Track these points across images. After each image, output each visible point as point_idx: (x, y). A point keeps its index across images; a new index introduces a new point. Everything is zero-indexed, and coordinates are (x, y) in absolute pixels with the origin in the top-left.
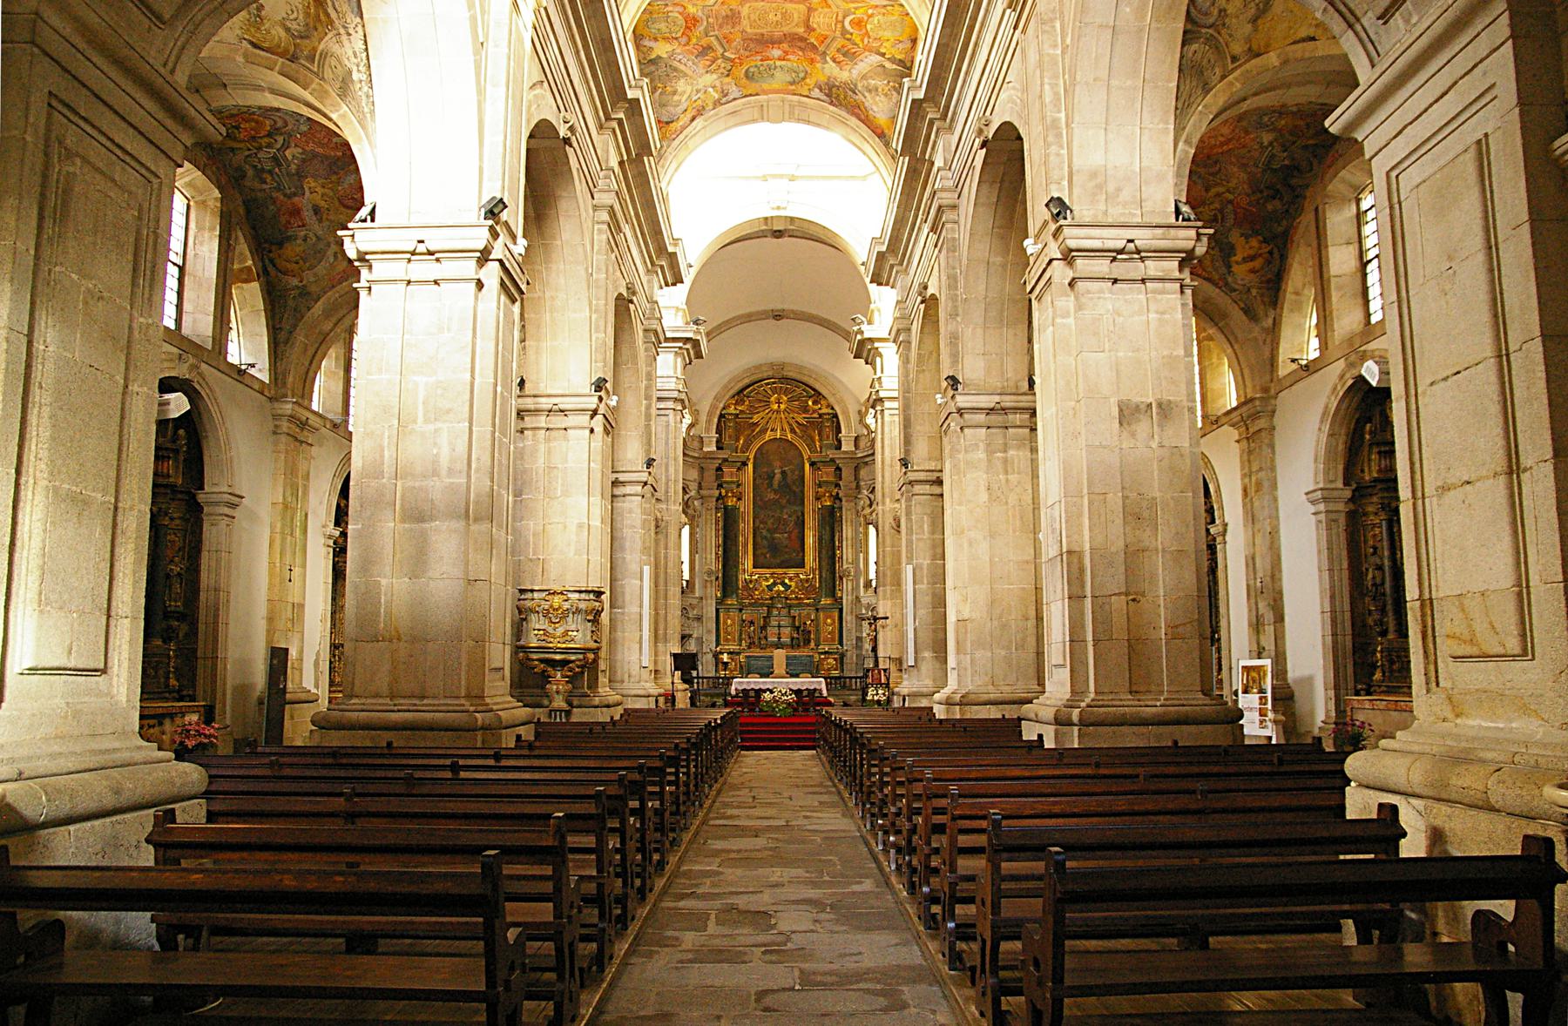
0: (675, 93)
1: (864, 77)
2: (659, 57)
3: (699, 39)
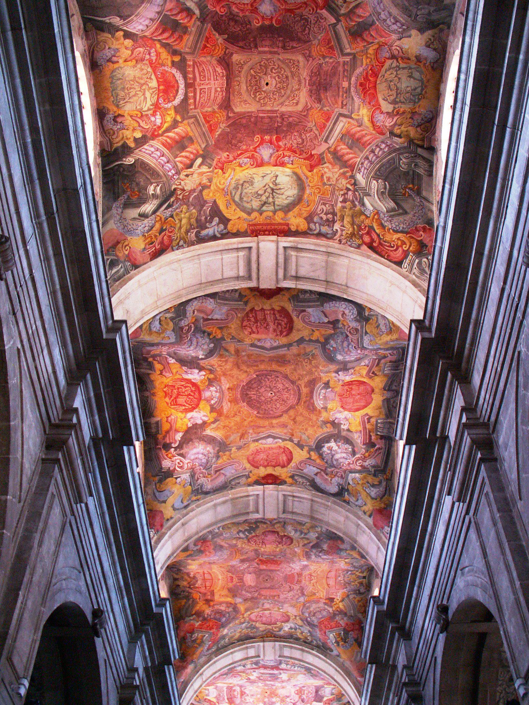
2: (421, 30)
3: (365, 52)
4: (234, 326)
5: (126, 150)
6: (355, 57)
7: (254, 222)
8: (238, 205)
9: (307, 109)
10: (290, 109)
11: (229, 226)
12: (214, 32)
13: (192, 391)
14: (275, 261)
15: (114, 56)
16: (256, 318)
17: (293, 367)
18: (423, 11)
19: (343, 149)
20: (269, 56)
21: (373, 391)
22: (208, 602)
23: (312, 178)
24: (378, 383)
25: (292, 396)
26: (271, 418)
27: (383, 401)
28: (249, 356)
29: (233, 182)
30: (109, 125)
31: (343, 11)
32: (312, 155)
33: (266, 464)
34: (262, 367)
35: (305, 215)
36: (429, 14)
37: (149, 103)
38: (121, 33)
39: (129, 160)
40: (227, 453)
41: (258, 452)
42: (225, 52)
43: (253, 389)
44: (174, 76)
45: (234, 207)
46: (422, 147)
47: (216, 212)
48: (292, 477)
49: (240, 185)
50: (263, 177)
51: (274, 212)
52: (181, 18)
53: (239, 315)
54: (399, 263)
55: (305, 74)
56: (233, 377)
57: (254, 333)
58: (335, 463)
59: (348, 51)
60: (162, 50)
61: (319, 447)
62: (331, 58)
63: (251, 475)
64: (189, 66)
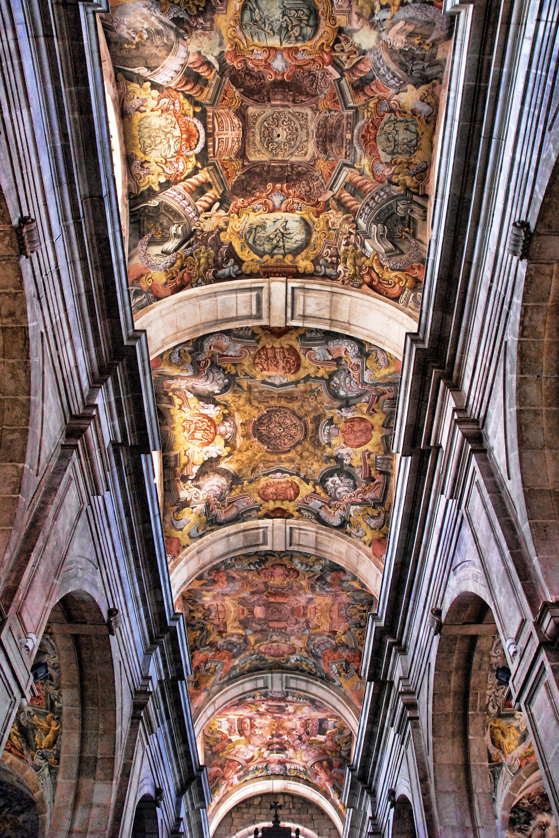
0: (411, 35)
1: (169, 49)
4: (247, 362)
5: (151, 193)
6: (357, 112)
7: (266, 264)
8: (251, 248)
9: (314, 159)
10: (299, 159)
11: (244, 268)
12: (232, 86)
13: (208, 426)
14: (284, 301)
15: (142, 106)
16: (266, 355)
17: (300, 403)
18: (418, 66)
19: (346, 196)
20: (281, 109)
21: (373, 427)
22: (220, 633)
23: (319, 223)
24: (378, 419)
25: (299, 432)
26: (280, 453)
27: (382, 438)
28: (261, 392)
29: (247, 226)
30: (137, 170)
31: (346, 67)
32: (318, 202)
33: (275, 497)
34: (272, 403)
35: (312, 258)
36: (423, 69)
37: (173, 150)
38: (148, 84)
39: (154, 203)
40: (240, 486)
41: (267, 486)
42: (241, 105)
43: (264, 424)
44: (195, 126)
45: (248, 249)
46: (417, 194)
47: (231, 253)
48: (299, 511)
49: (254, 229)
50: (274, 222)
51: (284, 255)
52: (202, 71)
53: (252, 353)
54: (396, 299)
55: (312, 126)
56: (245, 413)
57: (265, 370)
58: (338, 496)
59: (351, 105)
60: (185, 101)
61: (323, 481)
62: (336, 111)
63: (261, 508)
64: (209, 117)
